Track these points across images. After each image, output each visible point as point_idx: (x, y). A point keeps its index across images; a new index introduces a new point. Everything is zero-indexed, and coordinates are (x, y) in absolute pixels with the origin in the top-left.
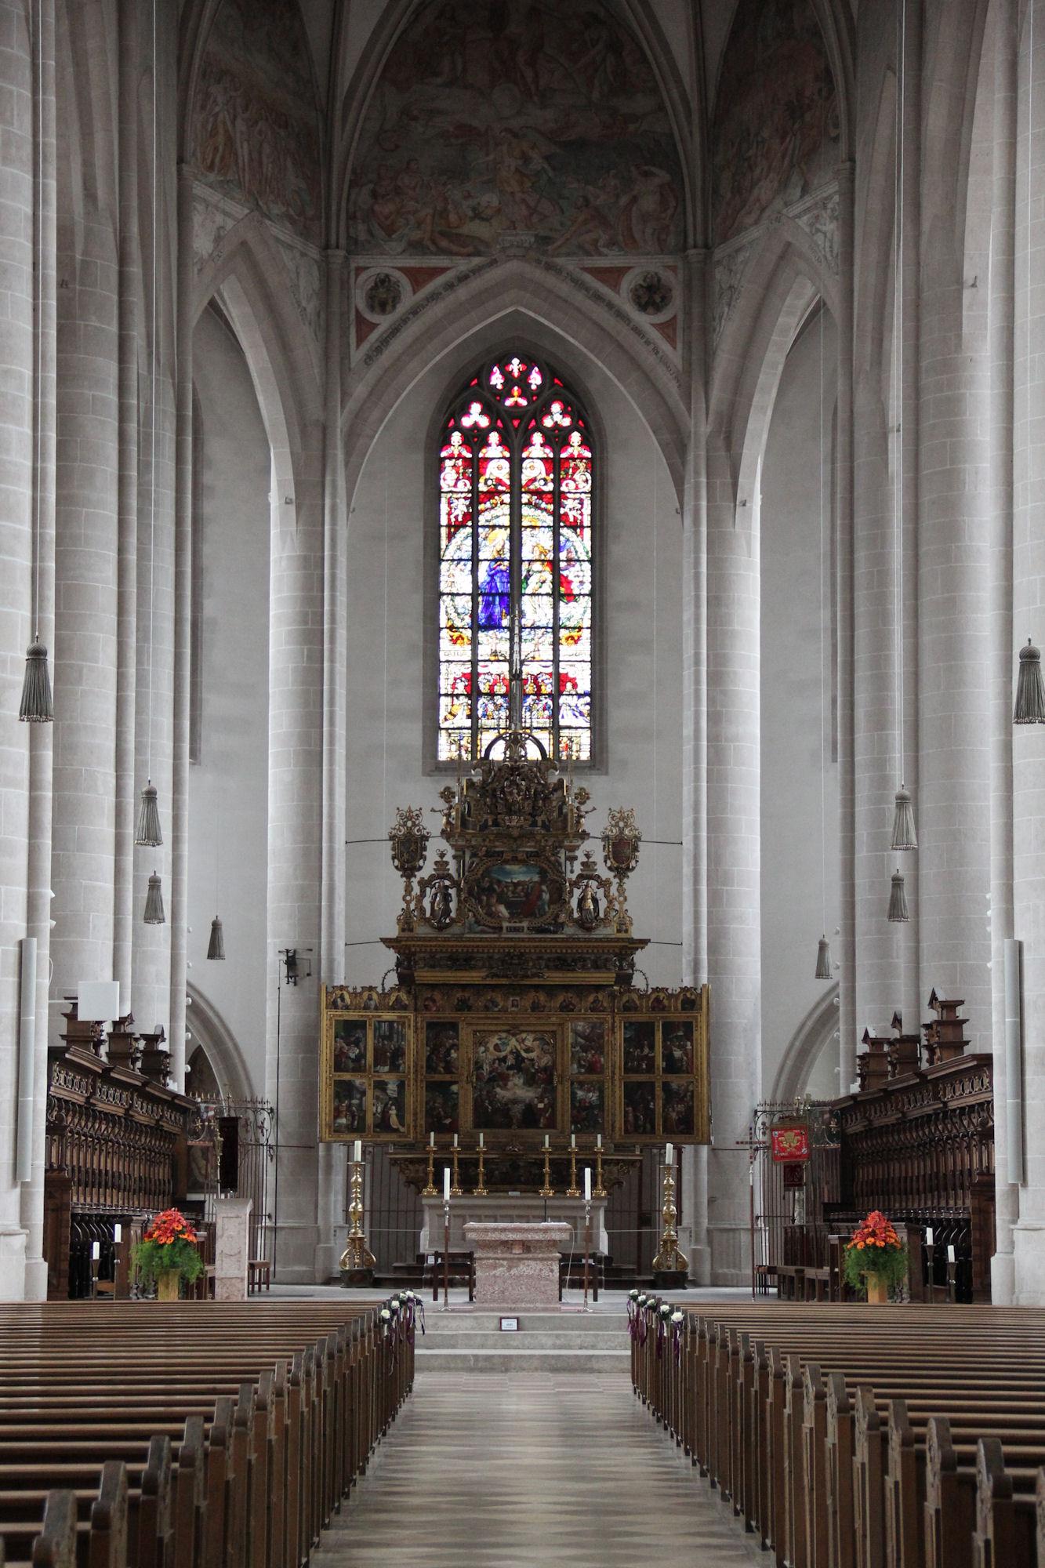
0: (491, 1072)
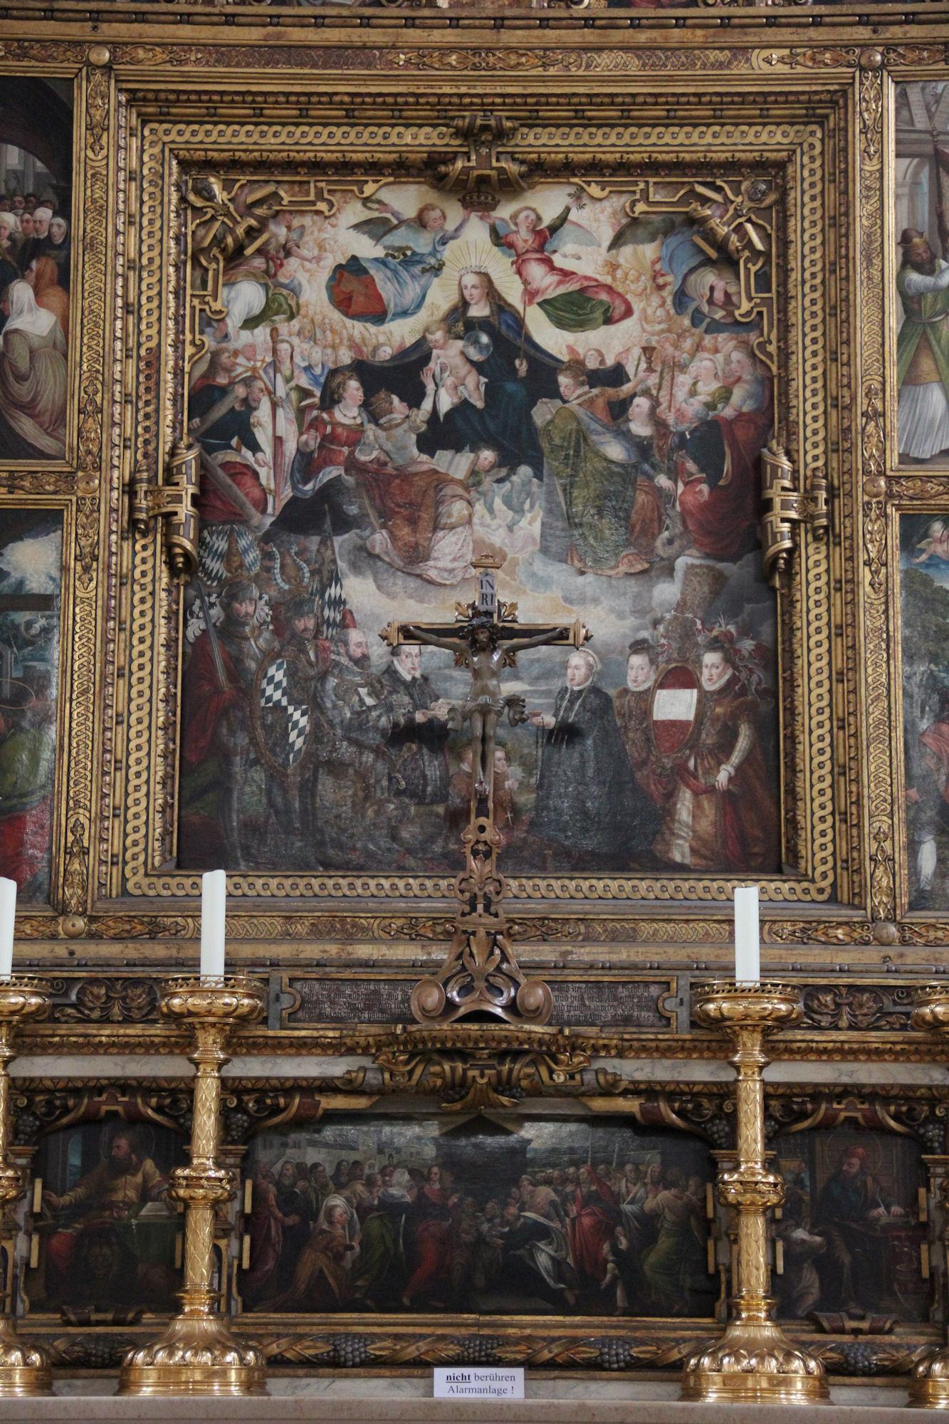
0: (307, 464)
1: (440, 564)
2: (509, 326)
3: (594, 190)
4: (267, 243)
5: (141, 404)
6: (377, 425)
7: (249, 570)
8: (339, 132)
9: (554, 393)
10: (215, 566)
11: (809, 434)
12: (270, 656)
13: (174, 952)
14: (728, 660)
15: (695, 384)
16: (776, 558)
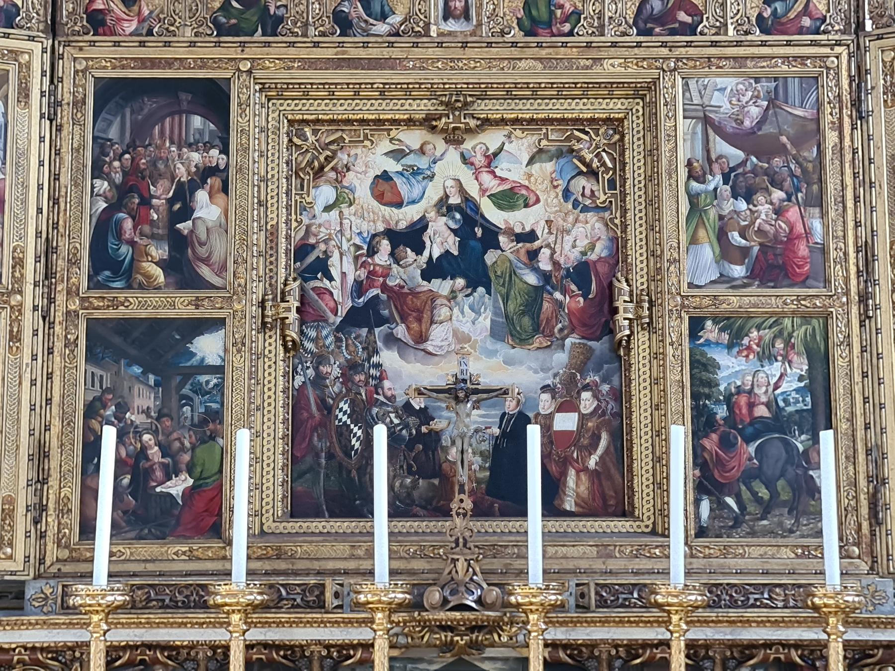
0: (359, 288)
1: (434, 343)
2: (471, 209)
3: (518, 133)
4: (336, 164)
5: (268, 257)
6: (399, 265)
7: (328, 348)
8: (376, 103)
9: (497, 246)
10: (309, 345)
11: (638, 270)
12: (338, 397)
13: (290, 566)
14: (595, 396)
15: (575, 241)
16: (621, 341)
